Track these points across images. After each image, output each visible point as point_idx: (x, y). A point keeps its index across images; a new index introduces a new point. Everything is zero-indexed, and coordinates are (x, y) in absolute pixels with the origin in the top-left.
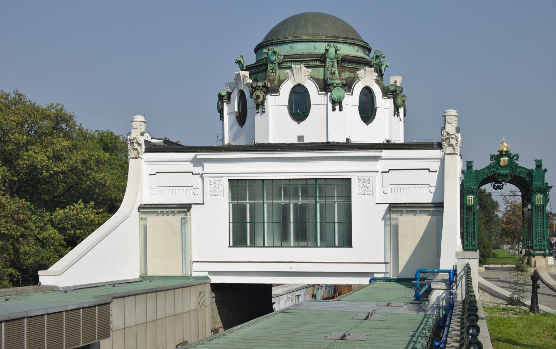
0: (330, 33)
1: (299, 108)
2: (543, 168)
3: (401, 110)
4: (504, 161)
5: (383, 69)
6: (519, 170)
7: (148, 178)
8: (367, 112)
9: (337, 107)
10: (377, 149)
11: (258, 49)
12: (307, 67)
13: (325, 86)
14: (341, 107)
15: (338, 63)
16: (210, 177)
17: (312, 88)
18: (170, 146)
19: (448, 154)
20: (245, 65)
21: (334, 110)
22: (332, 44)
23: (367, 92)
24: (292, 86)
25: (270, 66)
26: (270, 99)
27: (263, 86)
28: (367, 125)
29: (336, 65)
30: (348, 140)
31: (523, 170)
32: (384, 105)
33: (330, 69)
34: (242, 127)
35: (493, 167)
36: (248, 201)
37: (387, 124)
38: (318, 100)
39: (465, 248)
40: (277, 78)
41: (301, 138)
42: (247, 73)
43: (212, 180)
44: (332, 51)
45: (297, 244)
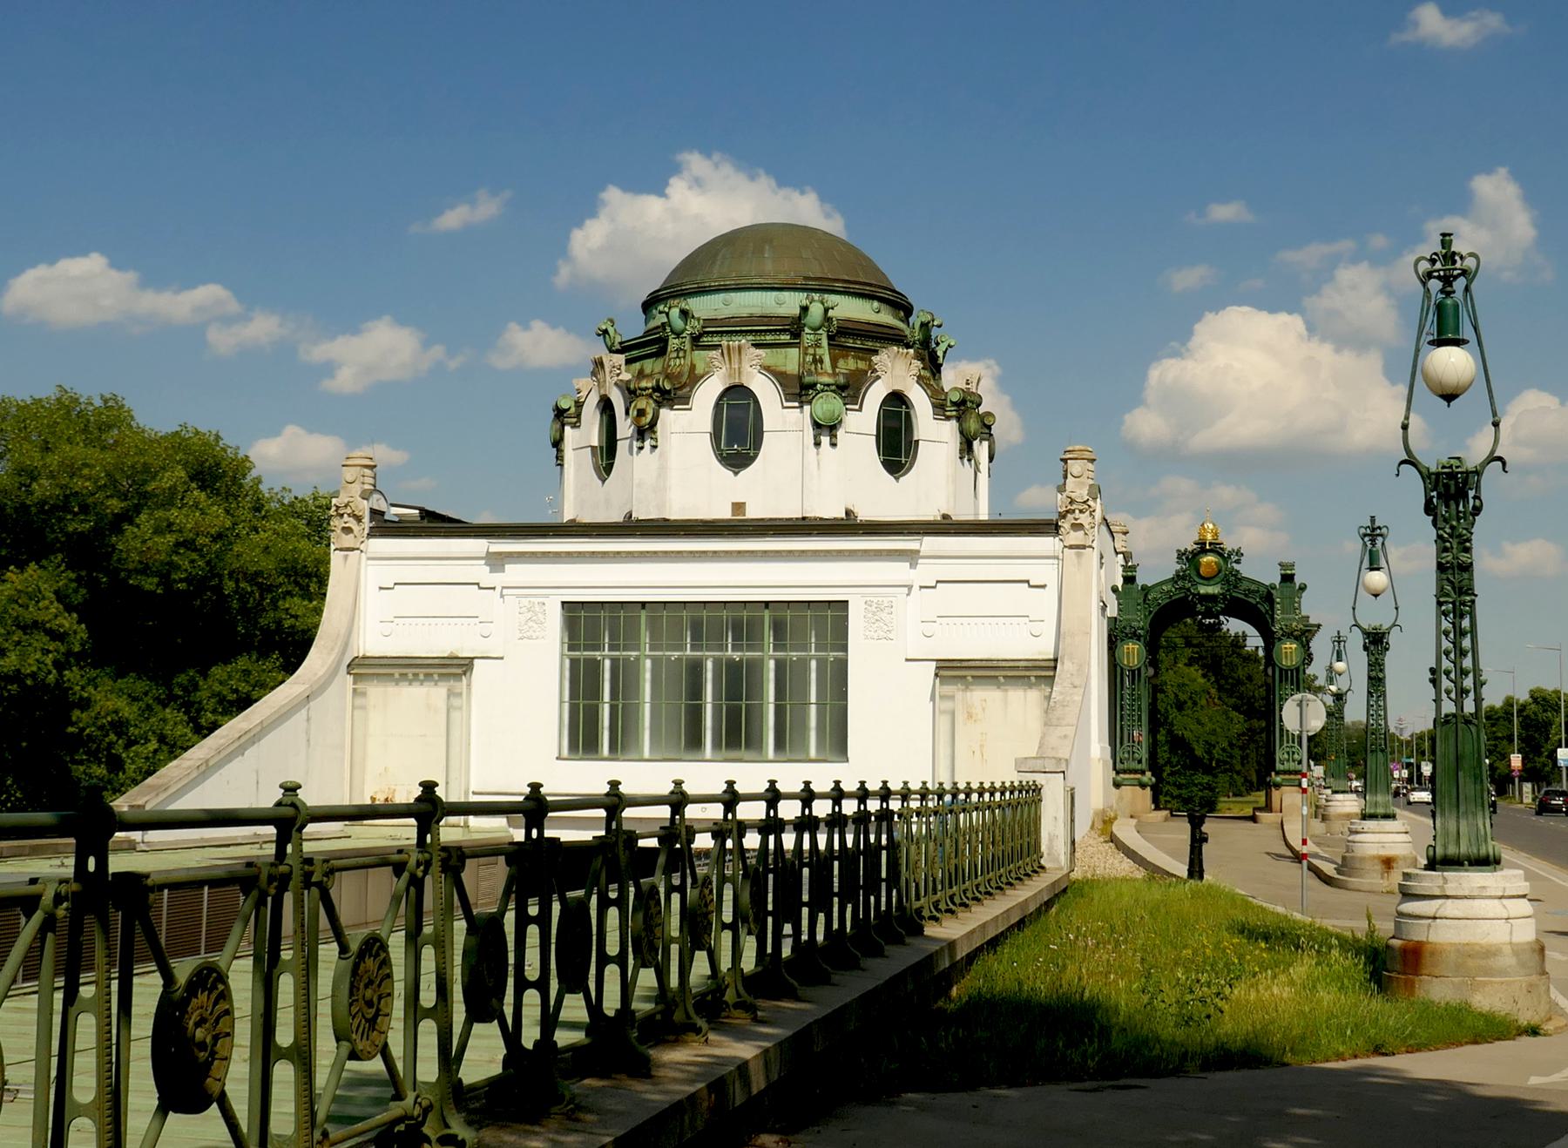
0: (815, 271)
1: (738, 437)
2: (1298, 581)
3: (981, 449)
4: (1208, 564)
5: (940, 353)
6: (1244, 585)
7: (378, 595)
8: (896, 446)
9: (825, 440)
10: (910, 534)
11: (649, 305)
12: (757, 346)
13: (799, 390)
14: (833, 436)
15: (830, 338)
16: (518, 596)
18: (434, 524)
19: (1071, 547)
21: (817, 444)
22: (816, 296)
23: (896, 399)
24: (721, 389)
25: (673, 343)
26: (670, 419)
28: (897, 479)
29: (825, 342)
30: (848, 512)
31: (1253, 587)
32: (935, 435)
33: (811, 351)
34: (604, 481)
35: (1183, 578)
36: (606, 652)
37: (940, 477)
38: (784, 423)
39: (1119, 766)
40: (686, 369)
41: (738, 507)
42: (620, 359)
43: (525, 601)
44: (816, 311)
45: (724, 753)
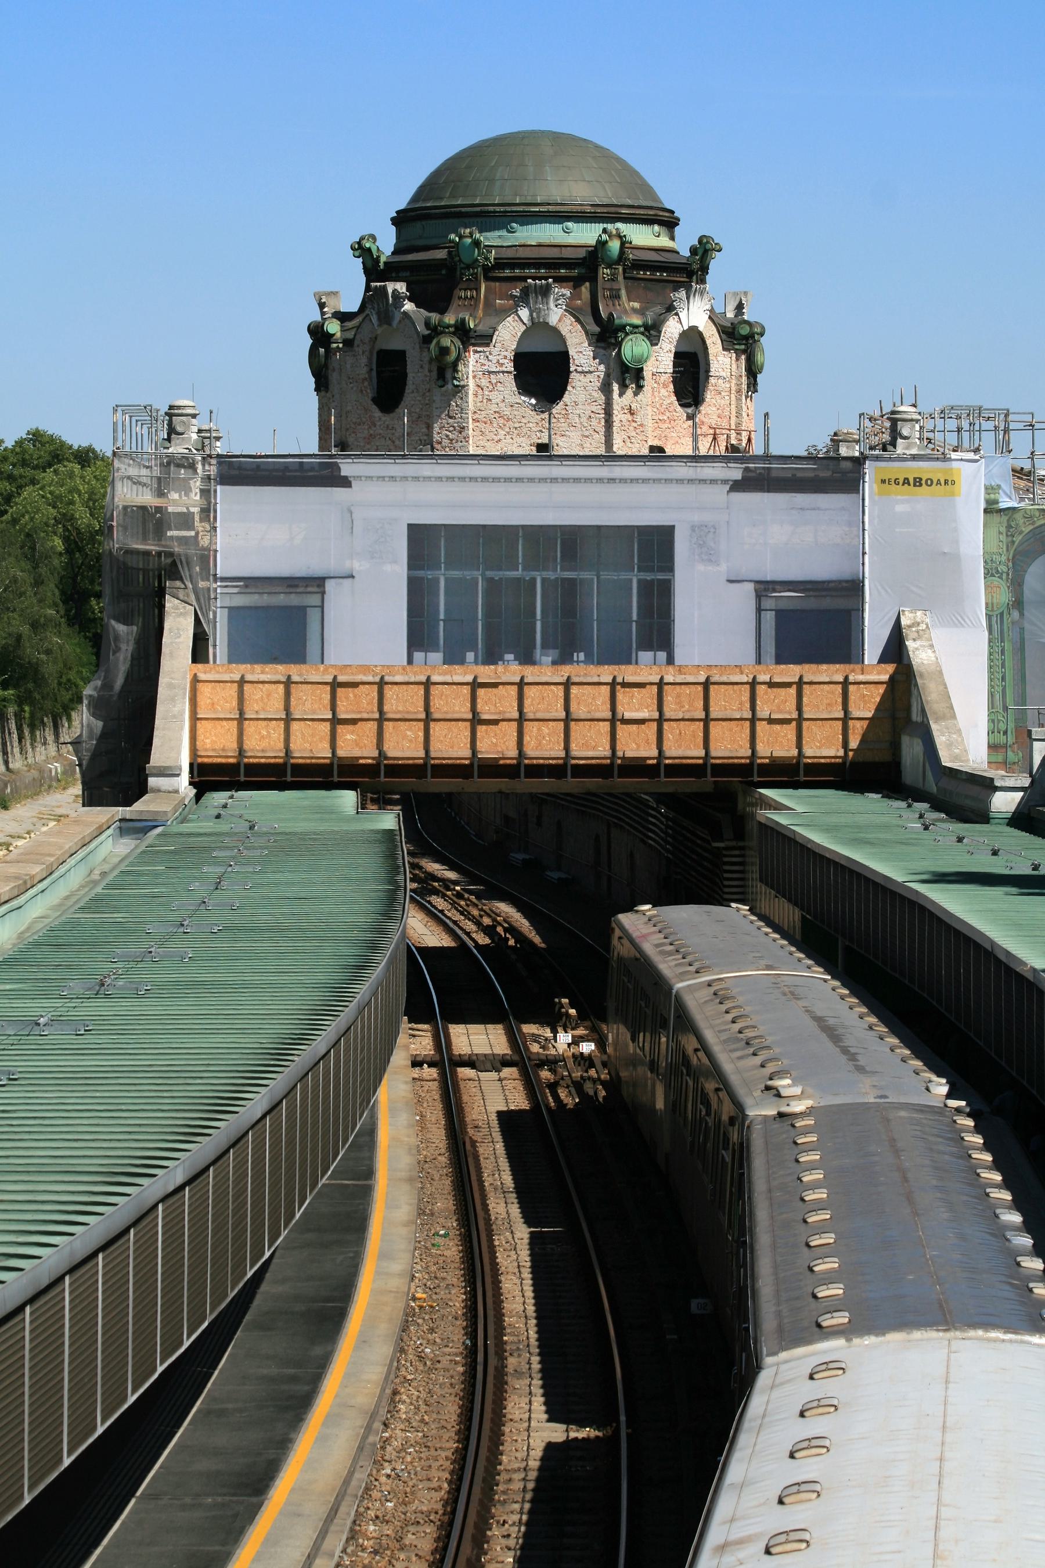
12: (558, 280)
20: (383, 259)
27: (455, 326)
29: (621, 278)
42: (401, 287)
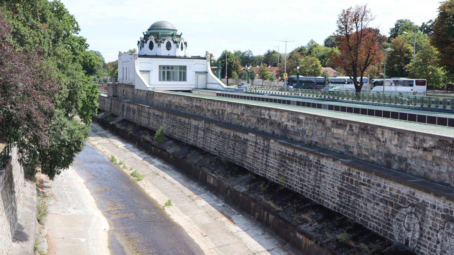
1: (169, 46)
8: (182, 48)
13: (175, 42)
17: (172, 42)
23: (182, 43)
26: (162, 44)
